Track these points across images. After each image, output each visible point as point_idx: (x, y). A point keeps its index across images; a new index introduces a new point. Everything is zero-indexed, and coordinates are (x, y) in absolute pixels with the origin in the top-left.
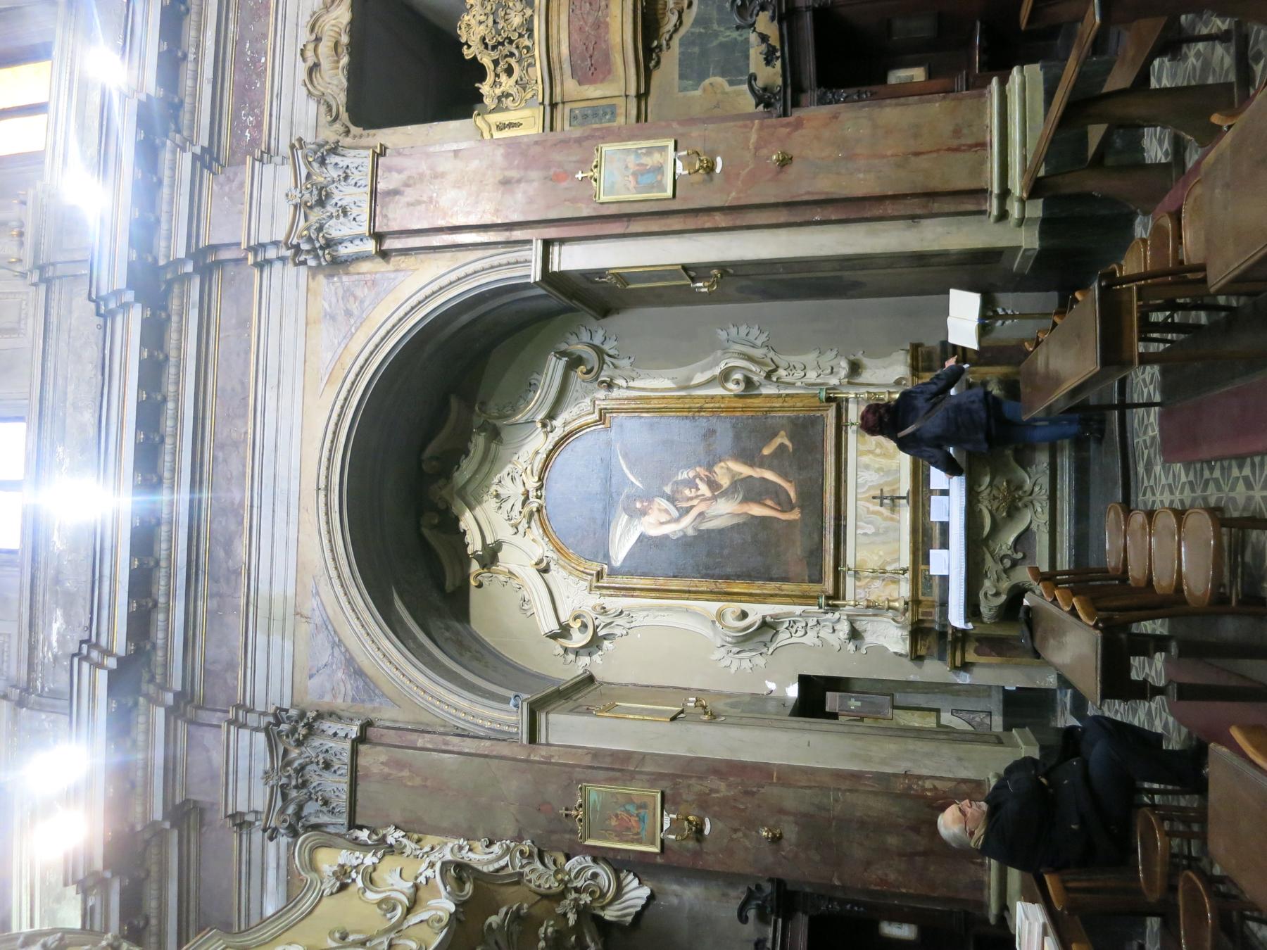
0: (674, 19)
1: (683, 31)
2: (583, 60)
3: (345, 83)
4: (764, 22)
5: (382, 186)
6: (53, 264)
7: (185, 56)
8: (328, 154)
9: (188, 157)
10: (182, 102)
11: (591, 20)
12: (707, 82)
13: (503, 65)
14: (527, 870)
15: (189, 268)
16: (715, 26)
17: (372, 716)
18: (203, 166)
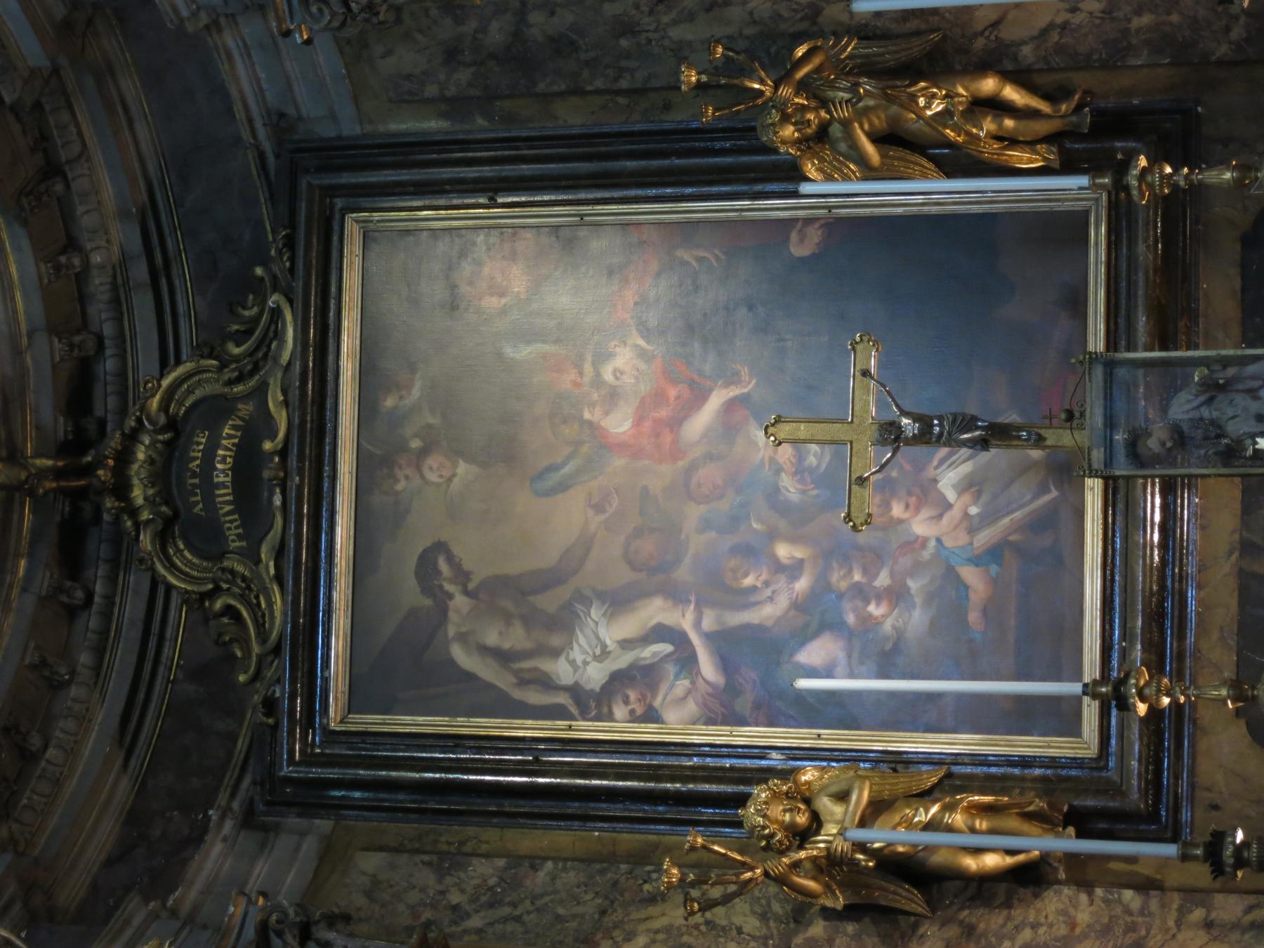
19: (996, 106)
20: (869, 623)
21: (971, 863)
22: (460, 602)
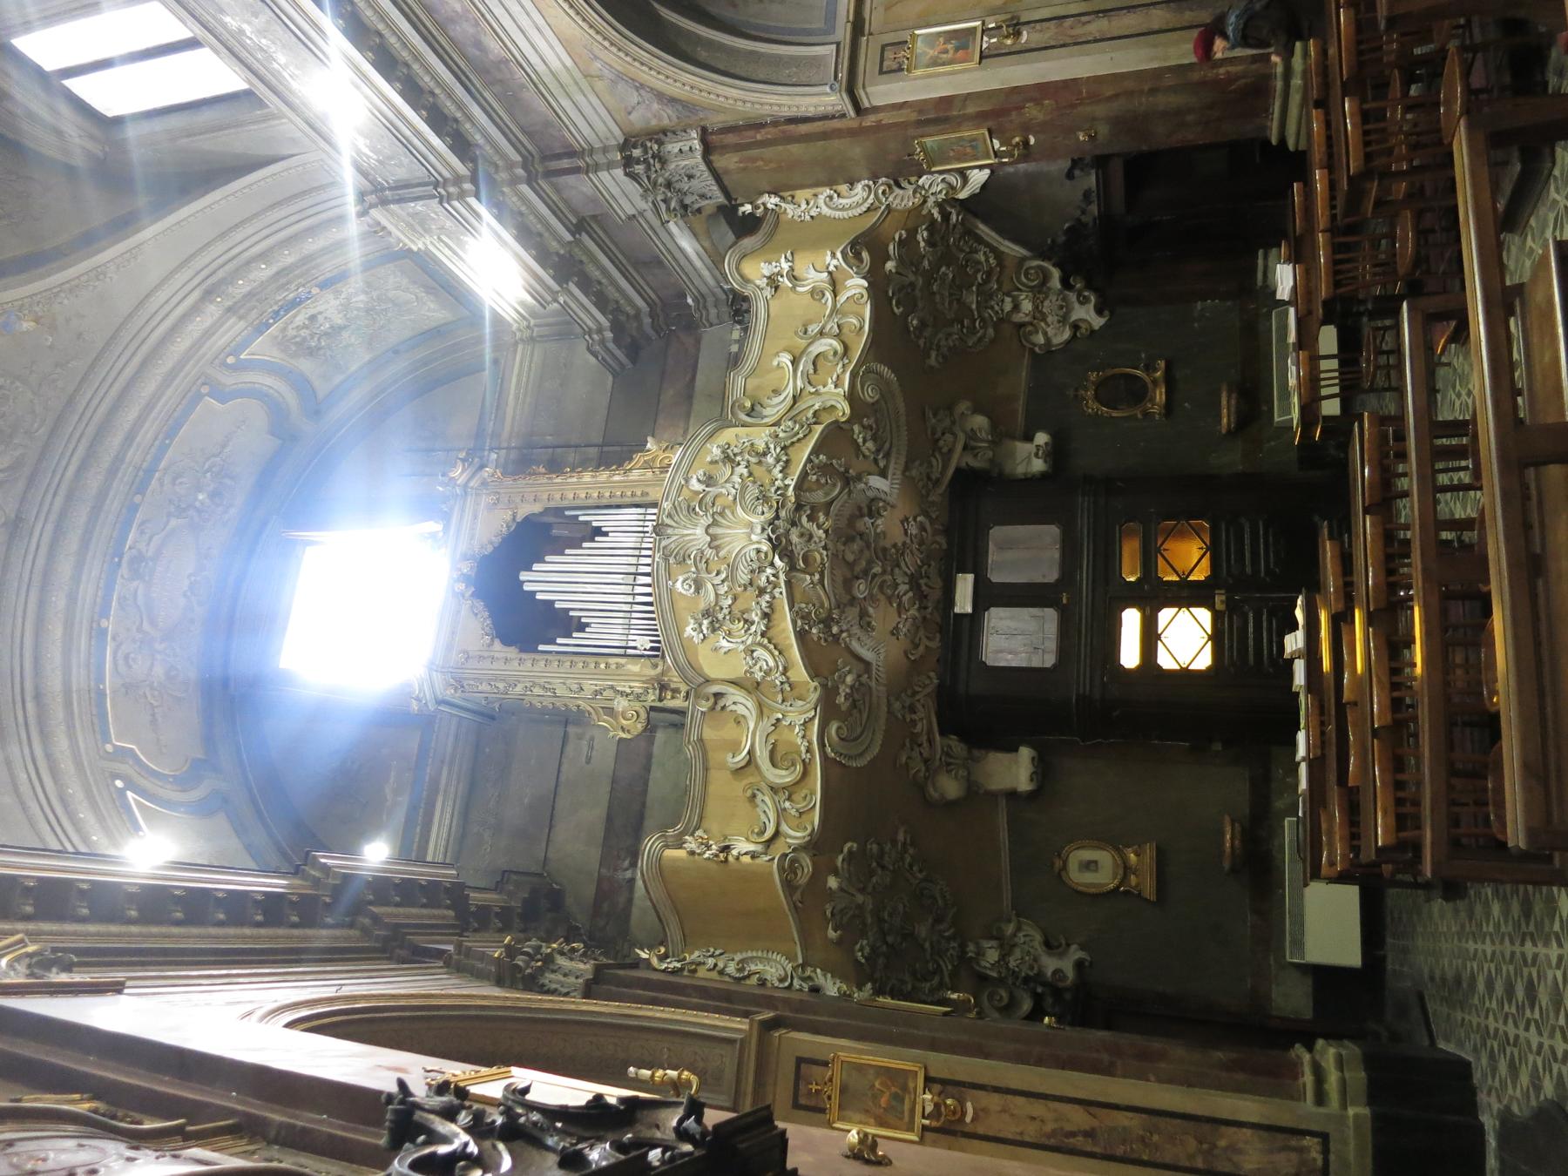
14: (891, 199)
17: (702, 124)
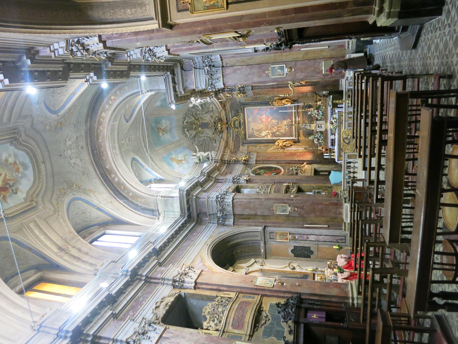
0: (264, 322)
1: (265, 325)
2: (236, 323)
3: (164, 312)
4: (290, 322)
5: (164, 335)
6: (45, 327)
7: (125, 293)
8: (152, 323)
9: (111, 312)
10: (117, 301)
11: (241, 314)
12: (271, 338)
13: (212, 319)
15: (90, 339)
16: (275, 326)
18: (113, 316)
19: (287, 101)
20: (281, 132)
21: (288, 145)
22: (255, 131)
